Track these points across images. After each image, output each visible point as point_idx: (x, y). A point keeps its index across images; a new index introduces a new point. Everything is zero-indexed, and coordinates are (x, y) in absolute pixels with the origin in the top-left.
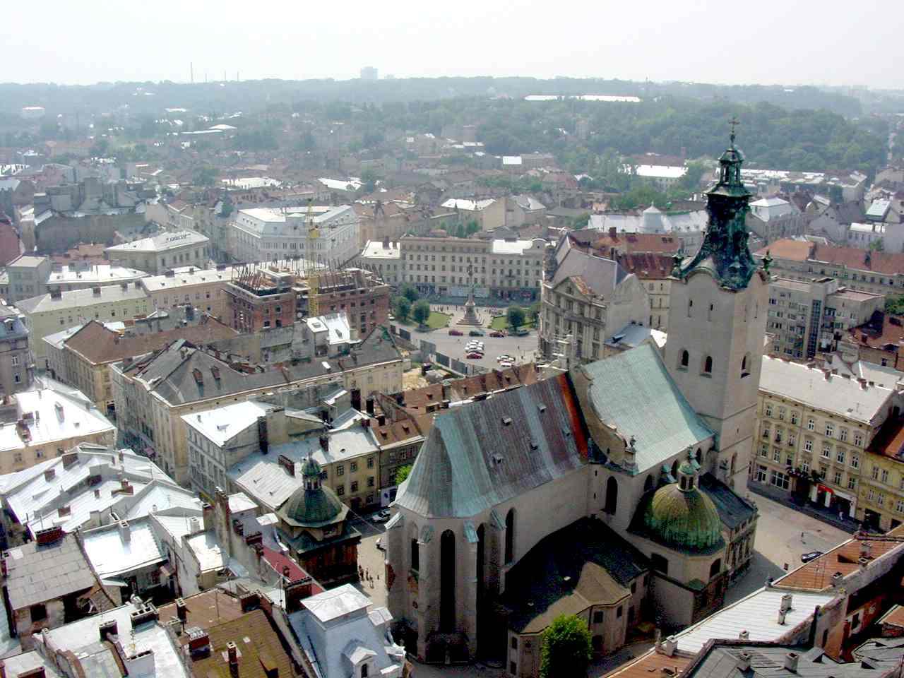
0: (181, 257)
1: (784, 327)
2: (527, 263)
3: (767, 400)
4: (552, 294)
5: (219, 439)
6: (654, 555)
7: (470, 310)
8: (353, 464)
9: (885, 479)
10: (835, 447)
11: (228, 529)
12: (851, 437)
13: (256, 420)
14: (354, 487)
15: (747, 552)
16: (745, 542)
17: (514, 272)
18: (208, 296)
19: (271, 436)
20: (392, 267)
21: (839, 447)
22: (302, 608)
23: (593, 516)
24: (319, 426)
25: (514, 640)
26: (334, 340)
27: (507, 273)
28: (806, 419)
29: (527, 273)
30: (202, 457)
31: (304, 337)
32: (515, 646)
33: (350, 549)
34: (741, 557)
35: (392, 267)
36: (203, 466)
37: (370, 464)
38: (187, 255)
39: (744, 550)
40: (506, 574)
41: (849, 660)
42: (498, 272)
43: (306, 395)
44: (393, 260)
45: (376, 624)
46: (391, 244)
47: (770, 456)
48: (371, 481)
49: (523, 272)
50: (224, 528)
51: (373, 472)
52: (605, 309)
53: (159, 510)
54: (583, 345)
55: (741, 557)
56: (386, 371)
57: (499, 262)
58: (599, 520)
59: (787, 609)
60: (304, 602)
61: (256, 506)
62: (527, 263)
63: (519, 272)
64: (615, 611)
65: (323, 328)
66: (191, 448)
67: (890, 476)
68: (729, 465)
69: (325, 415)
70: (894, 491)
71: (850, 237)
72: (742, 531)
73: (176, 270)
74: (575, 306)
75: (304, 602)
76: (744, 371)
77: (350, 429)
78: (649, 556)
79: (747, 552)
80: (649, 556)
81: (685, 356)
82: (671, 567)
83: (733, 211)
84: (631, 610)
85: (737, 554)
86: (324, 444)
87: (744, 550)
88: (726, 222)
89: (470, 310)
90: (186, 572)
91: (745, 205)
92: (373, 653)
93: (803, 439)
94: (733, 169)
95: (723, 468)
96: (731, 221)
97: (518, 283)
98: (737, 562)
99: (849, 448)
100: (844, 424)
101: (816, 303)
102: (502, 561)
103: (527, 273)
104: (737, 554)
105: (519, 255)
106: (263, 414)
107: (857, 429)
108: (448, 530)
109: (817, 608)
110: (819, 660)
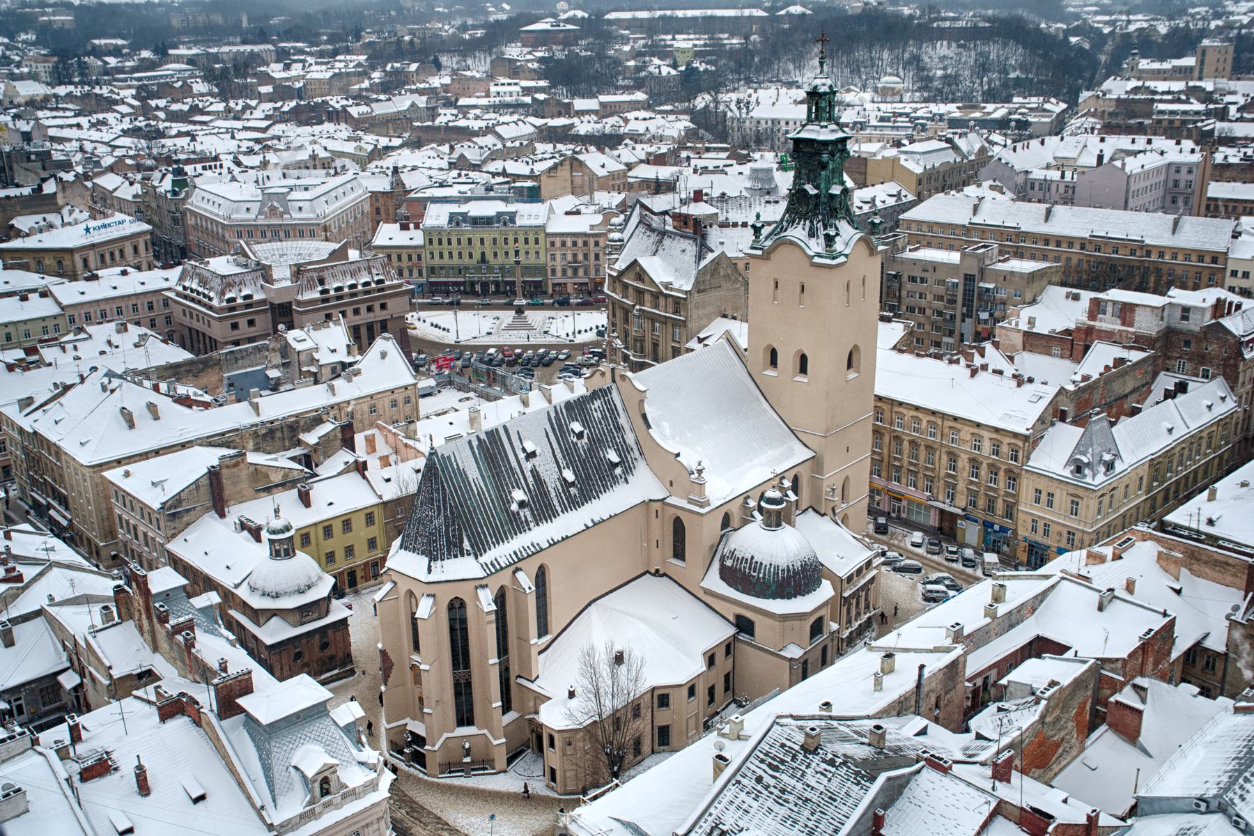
0: (112, 254)
1: (928, 312)
2: (597, 244)
3: (896, 409)
4: (617, 284)
5: (155, 500)
7: (520, 310)
8: (347, 522)
9: (1050, 504)
10: (985, 466)
11: (149, 618)
12: (1005, 449)
13: (206, 471)
14: (349, 551)
15: (867, 607)
18: (151, 308)
19: (228, 490)
20: (415, 258)
21: (990, 465)
22: (241, 710)
24: (296, 475)
26: (325, 358)
27: (570, 258)
28: (946, 431)
29: (597, 257)
30: (135, 528)
31: (283, 357)
32: (552, 745)
33: (339, 634)
35: (415, 258)
36: (137, 538)
37: (370, 519)
38: (122, 252)
39: (862, 605)
41: (967, 730)
42: (558, 257)
43: (279, 434)
44: (415, 247)
45: (342, 725)
46: (412, 226)
47: (904, 480)
48: (372, 543)
49: (592, 257)
50: (144, 616)
51: (374, 531)
52: (685, 299)
53: (57, 600)
54: (660, 348)
56: (395, 396)
57: (558, 242)
59: (887, 670)
60: (240, 701)
61: (184, 581)
62: (597, 244)
63: (586, 256)
64: (685, 692)
65: (308, 344)
66: (120, 517)
67: (1056, 501)
69: (307, 461)
71: (1032, 188)
73: (100, 273)
74: (647, 297)
75: (240, 701)
77: (339, 474)
79: (867, 607)
80: (731, 618)
81: (774, 353)
82: (757, 630)
83: (825, 157)
84: (711, 691)
85: (853, 612)
86: (305, 499)
87: (862, 605)
88: (817, 176)
89: (520, 310)
90: (93, 679)
91: (844, 150)
92: (335, 761)
93: (944, 457)
94: (823, 104)
96: (823, 173)
97: (586, 273)
99: (1003, 467)
100: (994, 436)
101: (969, 279)
103: (597, 257)
104: (853, 612)
105: (585, 235)
106: (216, 463)
107: (1013, 441)
109: (922, 667)
110: (923, 732)
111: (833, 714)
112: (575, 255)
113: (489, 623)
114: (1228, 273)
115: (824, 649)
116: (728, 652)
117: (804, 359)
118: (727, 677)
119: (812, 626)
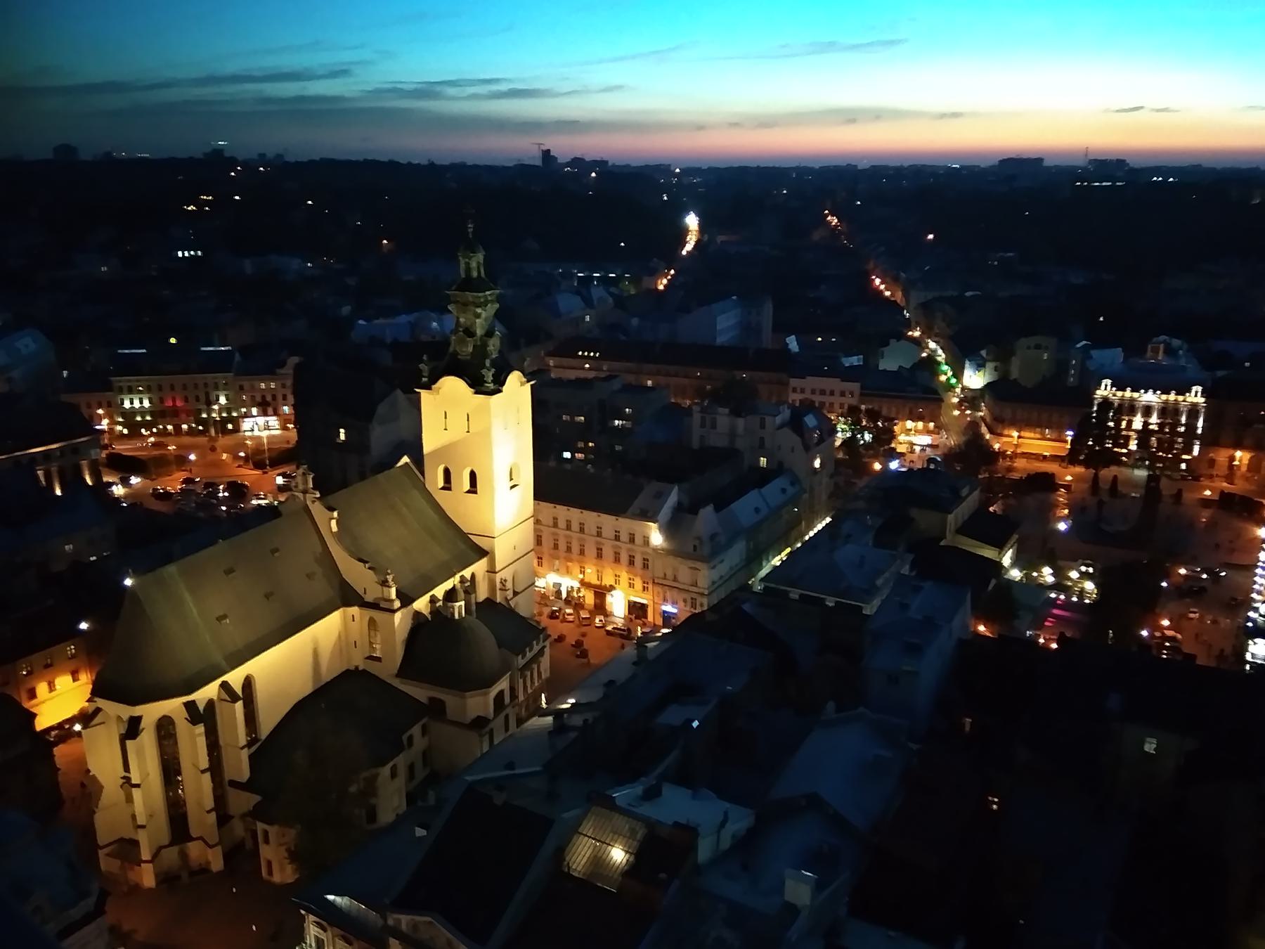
6: (431, 699)
16: (535, 666)
17: (269, 398)
23: (357, 668)
25: (266, 833)
32: (267, 841)
34: (532, 682)
40: (250, 757)
55: (532, 682)
58: (364, 671)
68: (509, 585)
70: (686, 587)
72: (529, 655)
76: (512, 483)
78: (424, 700)
84: (411, 768)
95: (503, 589)
98: (530, 691)
102: (243, 739)
108: (164, 717)
111: (517, 772)
112: (263, 397)
113: (200, 735)
114: (790, 390)
115: (507, 717)
116: (424, 734)
117: (473, 476)
118: (424, 754)
119: (495, 699)
